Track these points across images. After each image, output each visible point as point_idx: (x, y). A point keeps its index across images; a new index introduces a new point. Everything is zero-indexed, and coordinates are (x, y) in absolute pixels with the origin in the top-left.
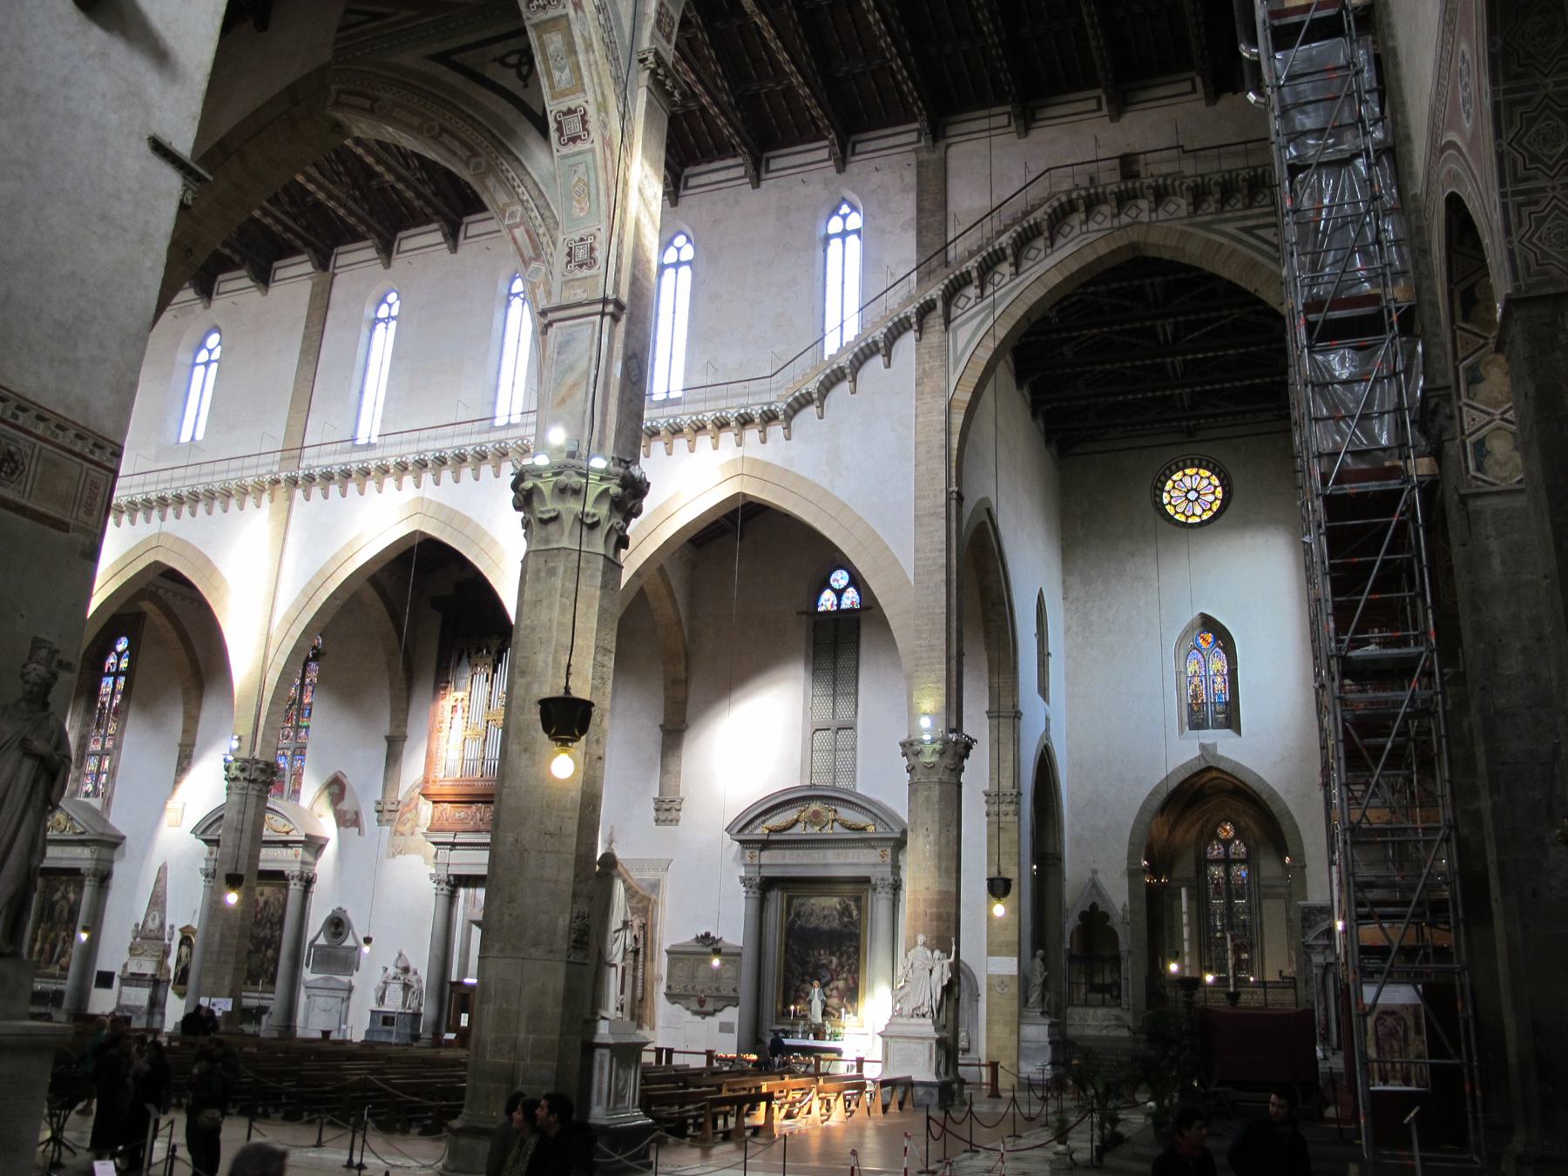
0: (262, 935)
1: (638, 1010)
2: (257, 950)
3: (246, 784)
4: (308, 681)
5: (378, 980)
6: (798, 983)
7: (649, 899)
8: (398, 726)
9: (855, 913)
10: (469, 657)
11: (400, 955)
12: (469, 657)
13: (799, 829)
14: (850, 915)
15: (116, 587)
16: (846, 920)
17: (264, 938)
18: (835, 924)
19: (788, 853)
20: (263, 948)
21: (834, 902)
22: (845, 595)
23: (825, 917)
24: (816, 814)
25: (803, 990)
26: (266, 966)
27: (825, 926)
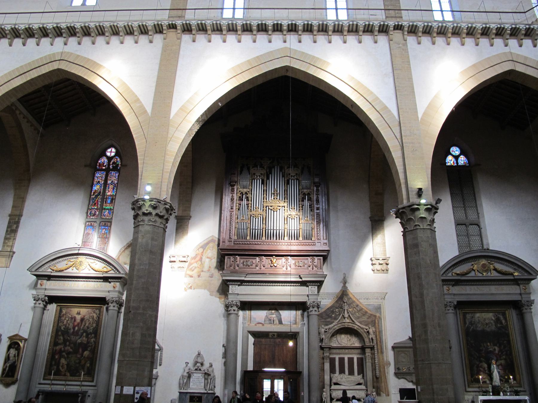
0: (79, 341)
1: (201, 386)
2: (76, 352)
3: (157, 219)
4: (109, 182)
5: (179, 370)
6: (477, 363)
7: (375, 316)
8: (185, 210)
9: (503, 321)
10: (249, 169)
11: (199, 354)
12: (249, 169)
13: (472, 274)
14: (501, 323)
15: (21, 82)
16: (499, 325)
17: (81, 344)
18: (493, 328)
19: (468, 287)
20: (81, 350)
21: (490, 316)
22: (453, 160)
23: (487, 324)
24: (484, 266)
25: (481, 367)
26: (83, 362)
27: (488, 329)
